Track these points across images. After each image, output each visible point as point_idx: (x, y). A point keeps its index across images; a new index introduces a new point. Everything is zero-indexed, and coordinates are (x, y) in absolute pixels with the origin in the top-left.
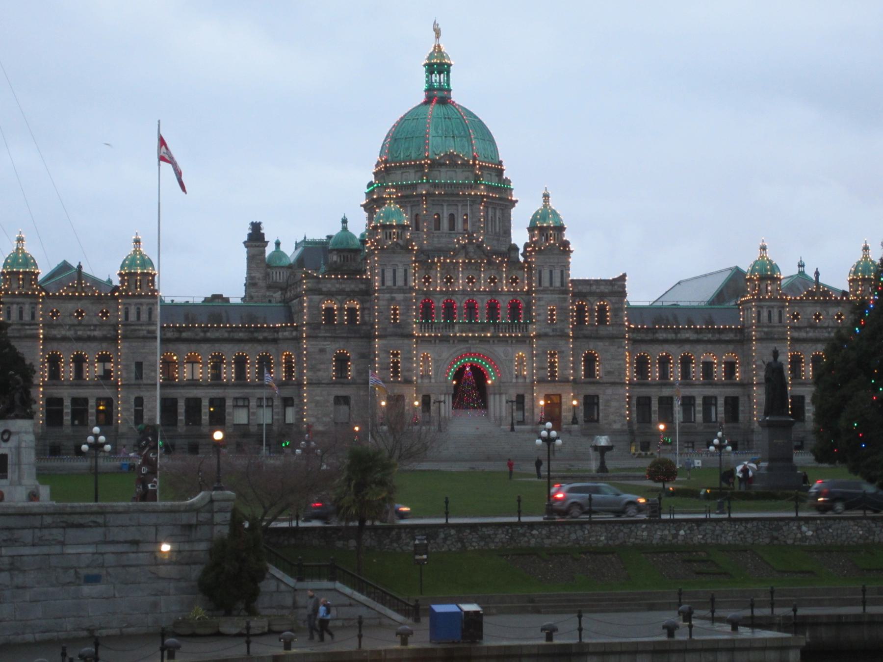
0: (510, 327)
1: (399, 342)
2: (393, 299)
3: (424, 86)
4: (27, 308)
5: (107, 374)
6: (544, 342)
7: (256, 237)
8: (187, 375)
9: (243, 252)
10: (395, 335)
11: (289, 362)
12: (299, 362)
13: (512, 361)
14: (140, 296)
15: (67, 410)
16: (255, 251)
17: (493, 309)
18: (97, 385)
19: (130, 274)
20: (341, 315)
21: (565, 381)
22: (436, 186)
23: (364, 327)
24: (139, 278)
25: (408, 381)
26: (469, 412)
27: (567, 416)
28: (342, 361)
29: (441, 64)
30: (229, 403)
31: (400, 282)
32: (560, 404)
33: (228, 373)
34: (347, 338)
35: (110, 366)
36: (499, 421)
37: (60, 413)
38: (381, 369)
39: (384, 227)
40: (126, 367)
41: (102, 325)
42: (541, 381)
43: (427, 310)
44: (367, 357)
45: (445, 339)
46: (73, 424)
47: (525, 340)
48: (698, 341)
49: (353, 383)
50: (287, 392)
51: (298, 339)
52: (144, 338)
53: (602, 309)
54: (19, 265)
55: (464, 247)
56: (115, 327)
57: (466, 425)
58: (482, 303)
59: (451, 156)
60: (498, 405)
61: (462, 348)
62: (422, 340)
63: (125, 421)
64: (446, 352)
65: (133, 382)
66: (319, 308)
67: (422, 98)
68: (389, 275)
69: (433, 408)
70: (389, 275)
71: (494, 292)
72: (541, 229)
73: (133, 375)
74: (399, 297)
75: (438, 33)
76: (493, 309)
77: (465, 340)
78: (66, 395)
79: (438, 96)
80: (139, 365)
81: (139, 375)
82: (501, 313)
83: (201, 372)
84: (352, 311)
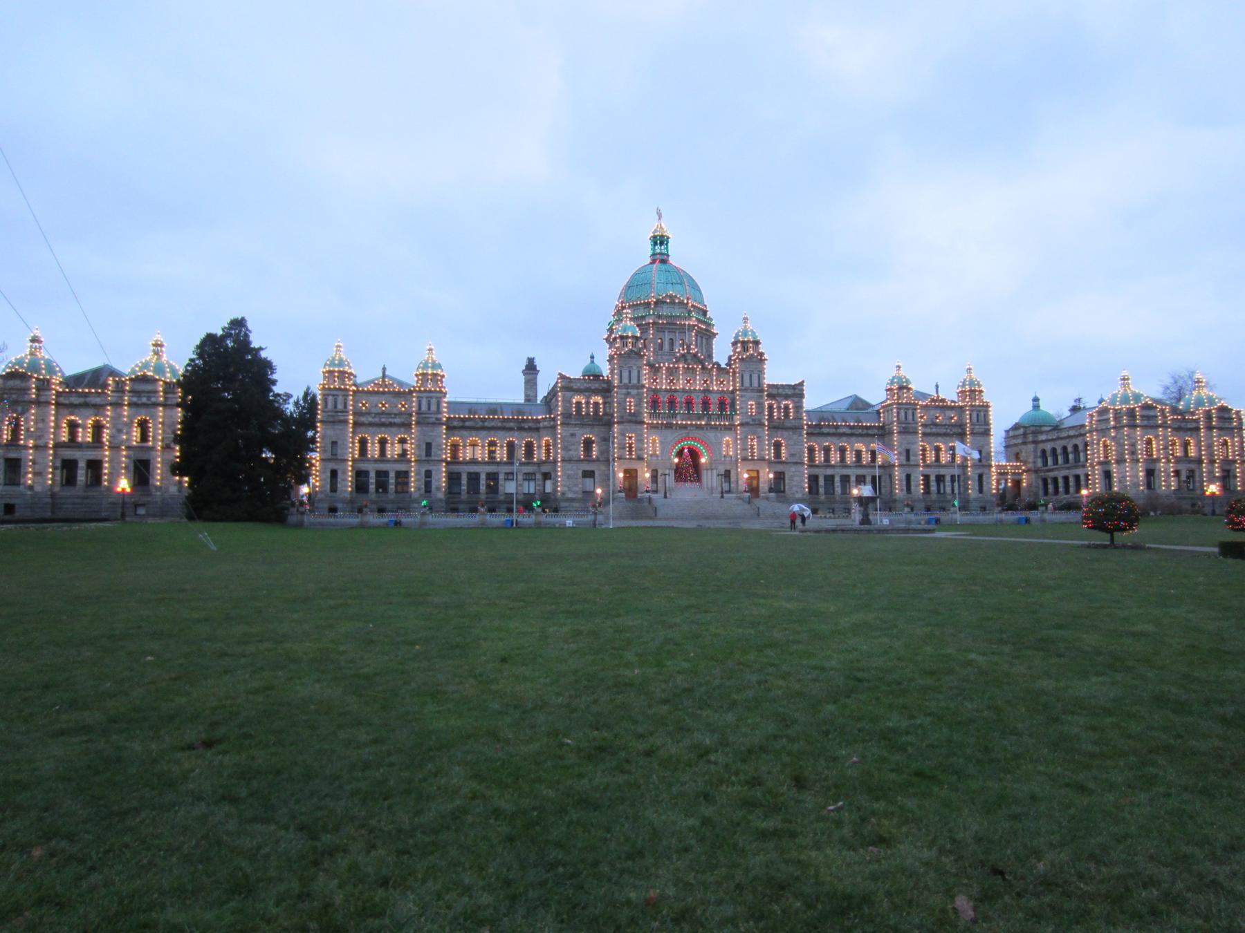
0: (720, 417)
1: (634, 426)
2: (628, 394)
3: (650, 253)
4: (340, 399)
5: (404, 452)
6: (746, 429)
7: (531, 368)
8: (469, 456)
9: (522, 378)
10: (630, 422)
11: (548, 445)
12: (555, 445)
13: (720, 444)
14: (430, 391)
15: (372, 480)
16: (530, 377)
17: (706, 404)
18: (396, 461)
19: (423, 374)
20: (588, 407)
21: (762, 459)
22: (659, 317)
23: (606, 418)
24: (431, 377)
25: (640, 458)
26: (687, 485)
27: (764, 486)
28: (588, 444)
29: (662, 236)
30: (501, 477)
31: (634, 381)
32: (758, 478)
33: (501, 454)
34: (592, 425)
35: (408, 446)
36: (712, 490)
37: (367, 484)
38: (619, 448)
39: (622, 337)
40: (418, 447)
41: (401, 414)
42: (744, 459)
43: (655, 404)
44: (606, 440)
45: (669, 426)
46: (377, 491)
47: (731, 428)
48: (852, 435)
49: (598, 460)
50: (545, 469)
51: (554, 427)
52: (433, 424)
53: (786, 407)
54: (335, 365)
55: (683, 355)
56: (411, 415)
57: (686, 493)
58: (698, 399)
59: (671, 297)
60: (710, 479)
61: (683, 433)
62: (651, 426)
63: (418, 489)
64: (671, 436)
65: (424, 458)
66: (571, 402)
67: (649, 260)
68: (625, 374)
69: (660, 480)
70: (625, 374)
71: (706, 391)
72: (743, 343)
73: (424, 453)
74: (634, 392)
75: (660, 215)
76: (706, 404)
77: (685, 427)
78: (372, 468)
79: (661, 259)
80: (429, 446)
81: (428, 453)
82: (712, 407)
83: (481, 454)
84: (596, 404)
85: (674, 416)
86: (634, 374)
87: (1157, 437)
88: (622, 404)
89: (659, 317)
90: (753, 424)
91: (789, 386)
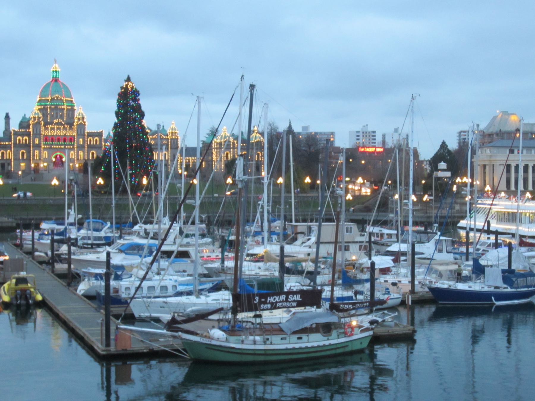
7: (7, 117)
9: (3, 122)
22: (53, 105)
25: (40, 159)
28: (23, 153)
31: (38, 132)
47: (73, 149)
50: (9, 162)
53: (96, 140)
59: (57, 97)
62: (44, 148)
67: (51, 80)
70: (35, 130)
71: (65, 135)
74: (38, 136)
85: (53, 145)
86: (38, 130)
87: (230, 152)
88: (34, 141)
89: (53, 105)
90: (81, 147)
91: (97, 132)
